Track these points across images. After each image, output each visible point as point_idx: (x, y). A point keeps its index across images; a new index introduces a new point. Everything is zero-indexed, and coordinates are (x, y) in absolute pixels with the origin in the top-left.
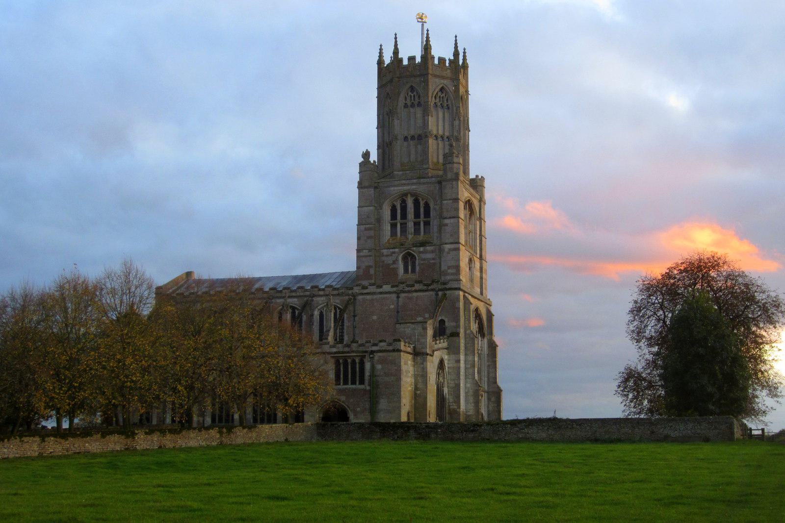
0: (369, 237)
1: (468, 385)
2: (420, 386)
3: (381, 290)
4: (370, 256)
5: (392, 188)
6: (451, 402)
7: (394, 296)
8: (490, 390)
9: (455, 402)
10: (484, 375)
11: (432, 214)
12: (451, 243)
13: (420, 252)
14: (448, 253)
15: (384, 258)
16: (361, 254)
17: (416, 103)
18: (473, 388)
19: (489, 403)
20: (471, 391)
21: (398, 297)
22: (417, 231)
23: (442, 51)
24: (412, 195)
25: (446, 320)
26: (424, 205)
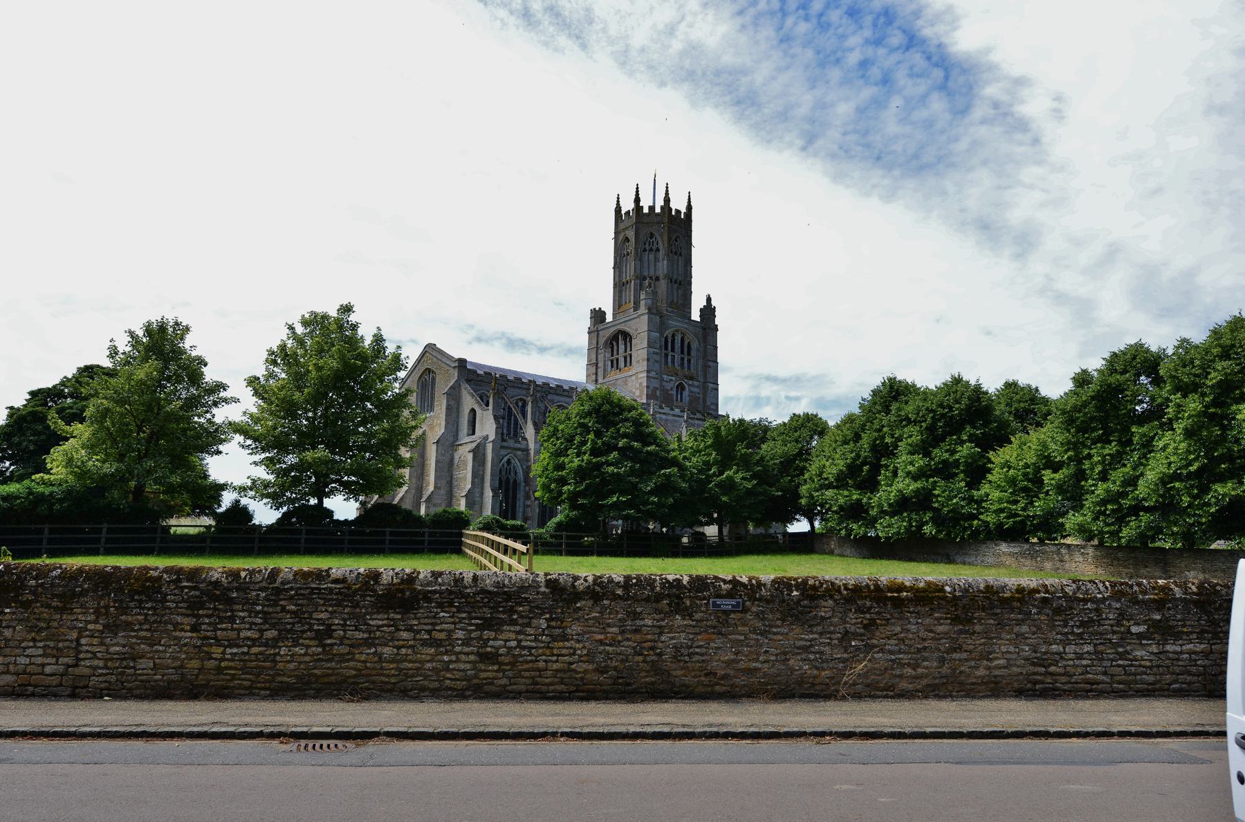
0: (656, 361)
11: (693, 353)
17: (654, 248)
22: (682, 364)
23: (678, 204)
24: (682, 333)
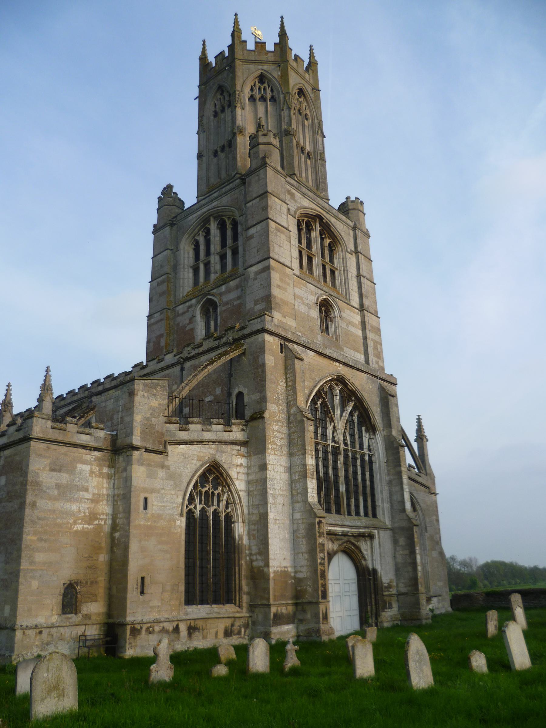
1: (297, 516)
2: (119, 521)
3: (162, 365)
4: (162, 320)
5: (191, 218)
6: (253, 552)
7: (177, 369)
8: (396, 525)
9: (260, 553)
10: (382, 499)
12: (259, 262)
13: (221, 294)
14: (255, 279)
15: (179, 319)
16: (153, 321)
18: (305, 521)
19: (395, 549)
20: (302, 527)
21: (182, 370)
25: (245, 392)
26: (231, 226)
